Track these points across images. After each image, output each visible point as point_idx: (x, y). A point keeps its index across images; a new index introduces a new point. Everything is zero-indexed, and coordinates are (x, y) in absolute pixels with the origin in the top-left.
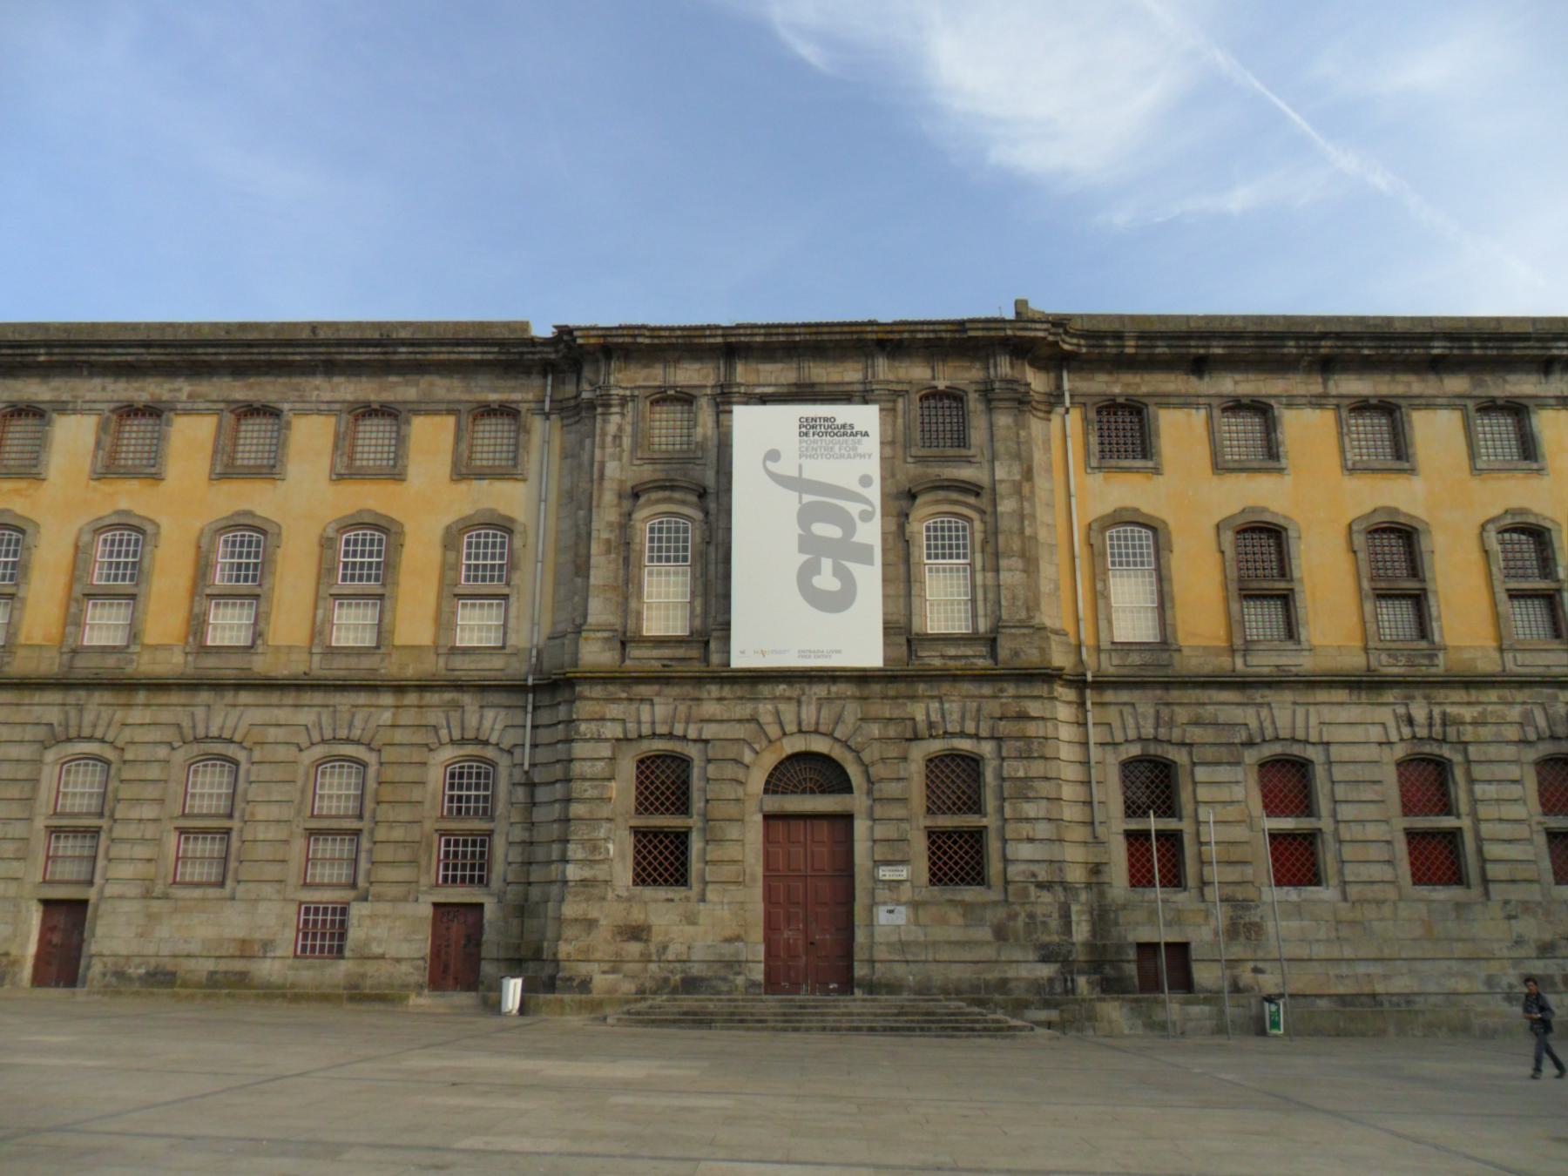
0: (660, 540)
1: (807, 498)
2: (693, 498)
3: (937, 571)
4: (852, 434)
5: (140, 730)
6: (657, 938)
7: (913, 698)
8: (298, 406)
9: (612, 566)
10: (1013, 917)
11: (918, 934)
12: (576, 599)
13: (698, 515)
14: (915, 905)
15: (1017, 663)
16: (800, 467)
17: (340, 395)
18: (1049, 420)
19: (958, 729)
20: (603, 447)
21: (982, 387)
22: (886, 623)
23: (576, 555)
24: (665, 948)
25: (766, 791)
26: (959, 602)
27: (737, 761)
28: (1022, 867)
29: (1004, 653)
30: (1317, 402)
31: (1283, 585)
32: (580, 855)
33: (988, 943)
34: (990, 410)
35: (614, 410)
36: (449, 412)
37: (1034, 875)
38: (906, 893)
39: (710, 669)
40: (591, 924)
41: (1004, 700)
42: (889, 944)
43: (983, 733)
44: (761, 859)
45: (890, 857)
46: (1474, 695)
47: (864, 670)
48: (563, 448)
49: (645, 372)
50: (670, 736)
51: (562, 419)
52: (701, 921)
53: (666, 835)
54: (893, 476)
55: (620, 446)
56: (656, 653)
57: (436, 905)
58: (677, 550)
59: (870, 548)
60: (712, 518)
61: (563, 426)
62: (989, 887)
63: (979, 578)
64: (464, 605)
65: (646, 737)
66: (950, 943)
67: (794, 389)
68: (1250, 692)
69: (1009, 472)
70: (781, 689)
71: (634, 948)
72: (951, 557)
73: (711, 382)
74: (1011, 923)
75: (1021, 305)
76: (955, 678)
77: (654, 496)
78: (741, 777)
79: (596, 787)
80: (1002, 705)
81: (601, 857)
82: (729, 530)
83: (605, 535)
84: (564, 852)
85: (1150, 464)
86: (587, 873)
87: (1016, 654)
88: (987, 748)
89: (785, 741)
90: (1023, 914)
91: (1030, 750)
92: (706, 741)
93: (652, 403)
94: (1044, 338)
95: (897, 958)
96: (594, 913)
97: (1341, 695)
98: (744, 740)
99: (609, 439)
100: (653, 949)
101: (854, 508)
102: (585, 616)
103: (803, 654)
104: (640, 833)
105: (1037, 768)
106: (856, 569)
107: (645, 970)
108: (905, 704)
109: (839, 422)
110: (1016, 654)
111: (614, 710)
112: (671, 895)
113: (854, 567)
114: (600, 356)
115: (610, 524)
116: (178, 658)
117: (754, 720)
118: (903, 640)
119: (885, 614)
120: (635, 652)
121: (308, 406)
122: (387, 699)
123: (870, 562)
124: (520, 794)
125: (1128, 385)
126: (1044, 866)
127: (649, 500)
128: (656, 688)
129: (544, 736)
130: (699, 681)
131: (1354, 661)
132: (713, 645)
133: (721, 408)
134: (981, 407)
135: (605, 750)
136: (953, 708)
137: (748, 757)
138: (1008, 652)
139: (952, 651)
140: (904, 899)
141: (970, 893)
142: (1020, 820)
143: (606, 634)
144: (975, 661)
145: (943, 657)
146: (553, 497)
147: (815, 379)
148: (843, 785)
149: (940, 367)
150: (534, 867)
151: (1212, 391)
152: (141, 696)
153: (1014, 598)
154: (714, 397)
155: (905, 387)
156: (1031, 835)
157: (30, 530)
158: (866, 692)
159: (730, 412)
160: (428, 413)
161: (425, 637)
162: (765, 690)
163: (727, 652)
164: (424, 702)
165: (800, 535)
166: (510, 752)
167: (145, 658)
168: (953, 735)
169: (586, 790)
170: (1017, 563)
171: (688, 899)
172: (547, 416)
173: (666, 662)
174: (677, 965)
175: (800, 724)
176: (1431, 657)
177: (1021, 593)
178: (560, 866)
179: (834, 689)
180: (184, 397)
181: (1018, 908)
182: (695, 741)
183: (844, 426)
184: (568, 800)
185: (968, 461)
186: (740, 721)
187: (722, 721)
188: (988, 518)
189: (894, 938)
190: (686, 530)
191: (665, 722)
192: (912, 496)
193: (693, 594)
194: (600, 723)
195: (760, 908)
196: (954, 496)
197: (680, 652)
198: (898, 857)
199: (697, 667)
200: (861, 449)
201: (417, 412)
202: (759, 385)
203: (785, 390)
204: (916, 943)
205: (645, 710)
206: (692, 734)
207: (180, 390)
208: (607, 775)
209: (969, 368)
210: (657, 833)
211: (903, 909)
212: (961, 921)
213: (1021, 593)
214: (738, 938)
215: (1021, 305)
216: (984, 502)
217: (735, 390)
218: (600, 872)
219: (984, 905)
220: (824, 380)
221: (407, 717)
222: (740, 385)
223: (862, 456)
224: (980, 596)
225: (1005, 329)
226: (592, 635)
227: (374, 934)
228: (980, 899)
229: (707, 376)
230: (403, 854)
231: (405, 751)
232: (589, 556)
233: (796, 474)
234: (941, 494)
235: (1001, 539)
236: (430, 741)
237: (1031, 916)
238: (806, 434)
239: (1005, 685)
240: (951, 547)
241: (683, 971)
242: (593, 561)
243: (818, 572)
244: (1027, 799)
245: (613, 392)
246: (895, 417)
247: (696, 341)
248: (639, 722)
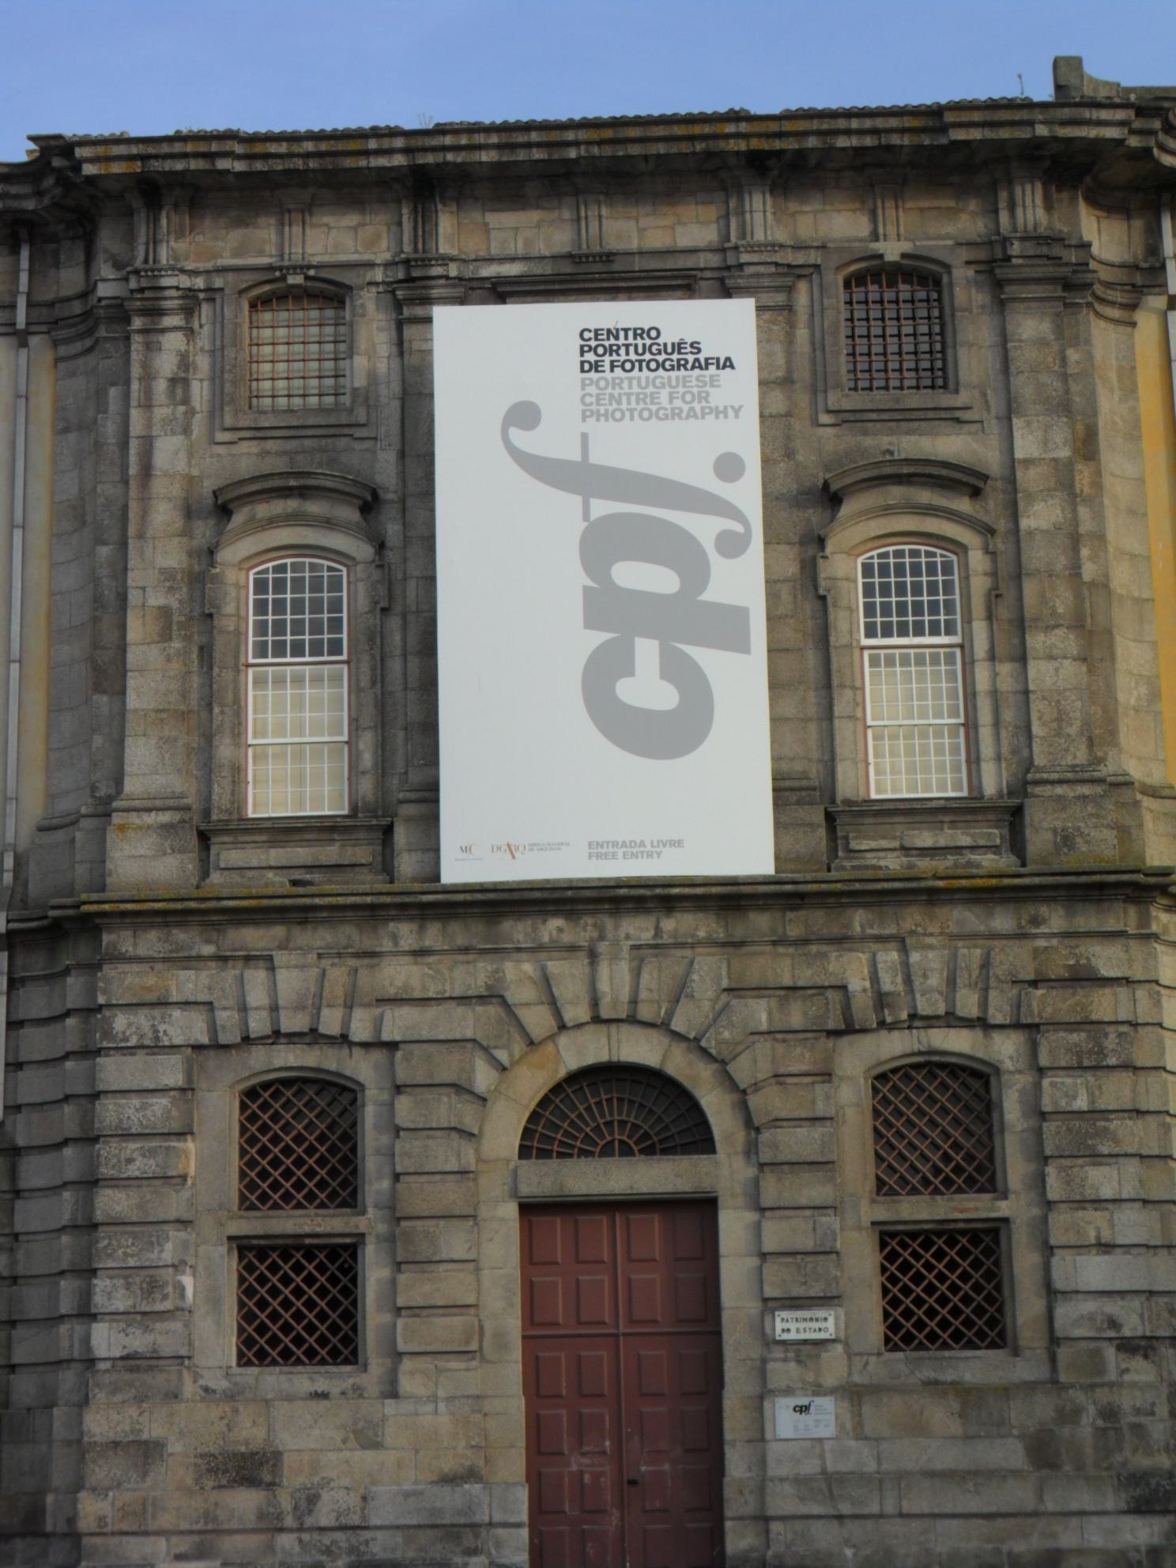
0: (279, 607)
1: (601, 508)
2: (348, 513)
3: (890, 661)
4: (697, 365)
6: (293, 1478)
7: (841, 941)
9: (176, 666)
10: (1070, 1416)
11: (862, 1457)
12: (98, 741)
13: (362, 550)
14: (854, 1394)
15: (1069, 862)
16: (585, 437)
18: (1134, 324)
19: (941, 1010)
20: (147, 405)
21: (982, 254)
22: (778, 777)
23: (95, 646)
24: (313, 1499)
25: (524, 1152)
26: (938, 731)
27: (460, 1088)
28: (1089, 1306)
29: (1038, 841)
32: (121, 1303)
33: (1015, 1473)
34: (1001, 305)
35: (169, 321)
37: (1113, 1324)
38: (834, 1367)
39: (396, 887)
40: (147, 1452)
41: (1042, 943)
42: (799, 1481)
43: (997, 1017)
44: (517, 1300)
45: (798, 1291)
47: (733, 882)
48: (59, 409)
49: (235, 236)
50: (313, 1036)
51: (56, 344)
52: (388, 1441)
53: (309, 1253)
54: (789, 454)
55: (186, 401)
56: (276, 856)
58: (316, 627)
59: (741, 614)
60: (391, 556)
61: (57, 360)
62: (1016, 1352)
63: (982, 676)
65: (261, 1040)
66: (932, 1475)
67: (567, 268)
69: (1045, 442)
70: (553, 927)
71: (245, 1502)
72: (919, 631)
73: (383, 253)
74: (1066, 1431)
75: (1066, 69)
76: (933, 896)
77: (263, 510)
78: (469, 1122)
79: (152, 1153)
80: (1036, 953)
81: (167, 1305)
82: (430, 580)
83: (156, 599)
84: (87, 1295)
86: (138, 1341)
87: (1066, 840)
88: (1006, 1049)
89: (563, 1040)
90: (1092, 1409)
91: (1101, 1052)
92: (393, 1046)
93: (253, 306)
94: (1120, 142)
95: (816, 1510)
96: (154, 1429)
98: (474, 1041)
99: (161, 386)
100: (285, 1502)
101: (704, 528)
102: (118, 780)
103: (598, 850)
104: (249, 1250)
105: (1116, 1091)
106: (707, 658)
107: (270, 1548)
108: (823, 956)
109: (668, 338)
110: (1066, 840)
111: (188, 983)
112: (321, 1385)
113: (706, 658)
114: (137, 203)
115: (168, 575)
117: (493, 996)
118: (819, 817)
119: (776, 759)
120: (229, 855)
123: (742, 645)
126: (1136, 1303)
127: (252, 519)
128: (279, 931)
129: (36, 1043)
130: (373, 913)
132: (401, 836)
133: (407, 312)
134: (980, 298)
135: (171, 1072)
136: (929, 961)
137: (483, 1077)
138: (1049, 836)
139: (925, 838)
140: (829, 1381)
142: (1082, 1203)
143: (165, 818)
144: (975, 857)
145: (905, 850)
146: (40, 517)
147: (613, 244)
149: (888, 211)
150: (20, 1332)
153: (1061, 718)
154: (390, 287)
155: (813, 257)
156: (1106, 1236)
158: (739, 932)
159: (428, 320)
162: (517, 930)
163: (434, 849)
165: (586, 589)
168: (931, 1021)
169: (130, 1161)
170: (1065, 641)
171: (359, 1391)
172: (21, 339)
173: (297, 875)
174: (339, 1536)
175: (595, 1003)
177: (1075, 707)
178: (79, 1328)
179: (669, 924)
181: (1080, 1397)
182: (365, 1045)
183: (679, 347)
184: (91, 1183)
185: (954, 418)
186: (463, 1000)
187: (424, 1001)
188: (1000, 544)
189: (810, 1467)
190: (335, 585)
191: (300, 1007)
192: (831, 498)
193: (355, 725)
194: (157, 1012)
195: (514, 1407)
196: (925, 496)
197: (330, 853)
198: (816, 1290)
199: (368, 883)
200: (717, 398)
202: (490, 260)
203: (547, 269)
204: (860, 1477)
205: (256, 977)
206: (360, 1030)
208: (176, 1126)
209: (952, 213)
210: (289, 1248)
211: (826, 1405)
212: (955, 1427)
213: (1075, 707)
214: (471, 1475)
215: (1066, 69)
216: (991, 509)
217: (437, 271)
218: (165, 1338)
219: (1006, 1392)
220: (634, 245)
222: (446, 260)
223: (720, 412)
224: (985, 716)
225: (1031, 123)
226: (134, 819)
228: (997, 1377)
229: (372, 243)
232: (122, 647)
233: (577, 457)
234: (896, 494)
235: (1030, 588)
237: (1110, 1413)
238: (596, 367)
239: (1044, 910)
240: (918, 609)
241: (352, 1550)
242: (133, 657)
243: (630, 672)
244: (1096, 1158)
245: (166, 282)
246: (791, 325)
247: (348, 163)
248: (243, 1008)
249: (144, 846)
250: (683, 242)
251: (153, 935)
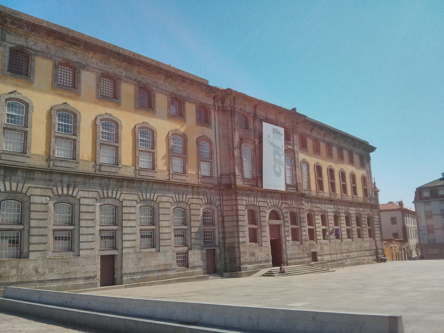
1: (275, 149)
10: (304, 247)
36: (194, 103)
57: (206, 250)
61: (218, 115)
109: (278, 131)
124: (220, 219)
137: (266, 211)
157: (78, 115)
160: (189, 102)
166: (217, 207)
193: (252, 168)
201: (187, 101)
207: (122, 72)
236: (201, 203)
237: (306, 247)
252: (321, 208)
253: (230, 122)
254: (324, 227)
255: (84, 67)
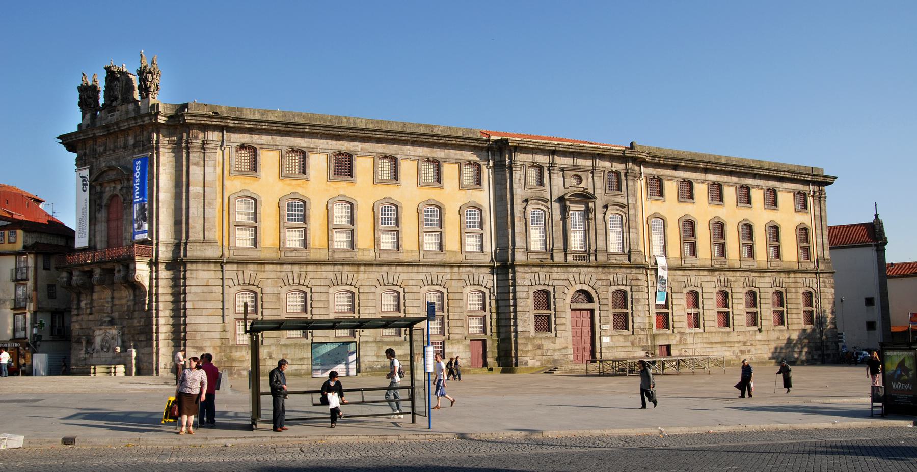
5: (364, 281)
6: (545, 347)
8: (403, 156)
10: (635, 339)
14: (612, 336)
17: (417, 154)
28: (637, 324)
29: (632, 260)
30: (703, 181)
31: (693, 239)
36: (456, 163)
46: (734, 274)
56: (537, 257)
62: (628, 330)
64: (468, 236)
68: (686, 272)
71: (539, 352)
83: (519, 215)
85: (663, 199)
86: (524, 329)
88: (628, 289)
97: (706, 273)
111: (528, 276)
115: (520, 211)
116: (373, 254)
121: (406, 157)
122: (448, 270)
125: (657, 172)
130: (552, 266)
131: (708, 263)
136: (620, 276)
137: (566, 291)
141: (625, 332)
143: (522, 250)
148: (590, 299)
151: (678, 176)
152: (362, 268)
160: (449, 163)
161: (457, 248)
164: (460, 271)
166: (490, 289)
167: (360, 253)
176: (726, 262)
180: (360, 150)
189: (607, 346)
195: (570, 338)
201: (445, 162)
213: (635, 240)
216: (625, 210)
221: (456, 277)
222: (557, 164)
227: (453, 351)
230: (459, 324)
231: (456, 288)
237: (640, 338)
247: (546, 148)
249: (520, 254)
250: (587, 165)
251: (522, 268)
252: (686, 282)
253: (508, 180)
254: (693, 310)
255: (312, 150)
